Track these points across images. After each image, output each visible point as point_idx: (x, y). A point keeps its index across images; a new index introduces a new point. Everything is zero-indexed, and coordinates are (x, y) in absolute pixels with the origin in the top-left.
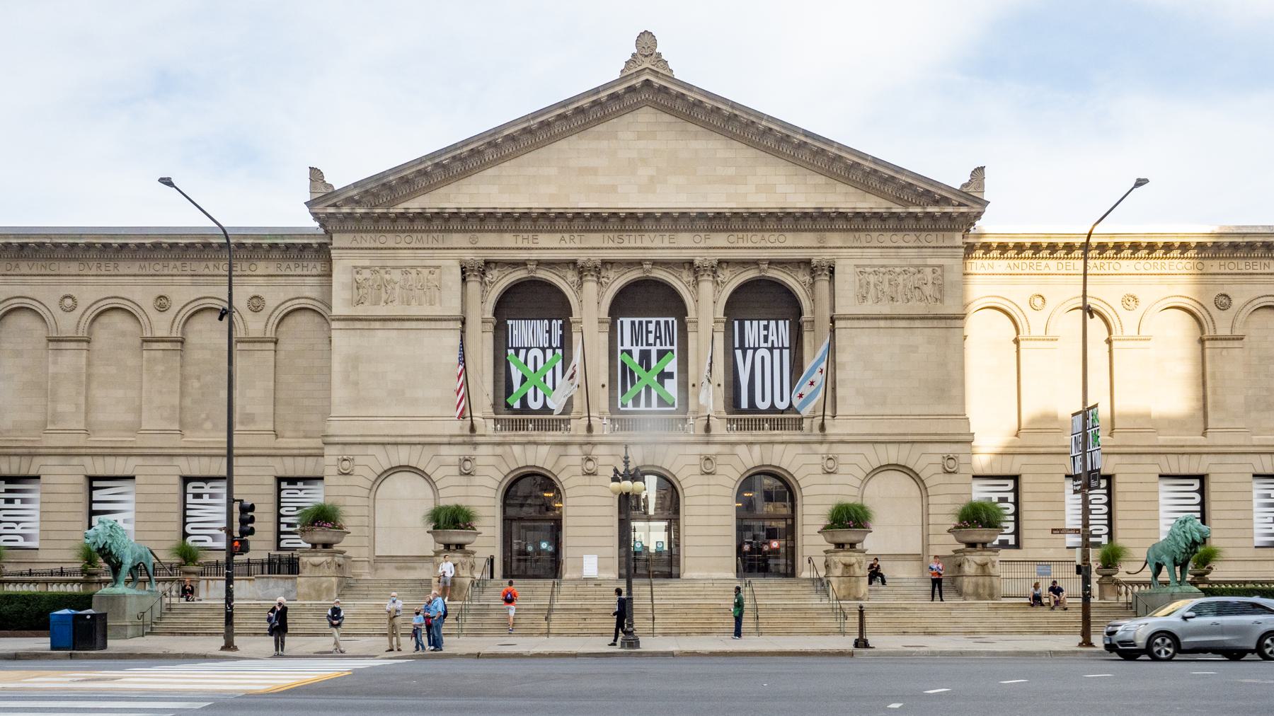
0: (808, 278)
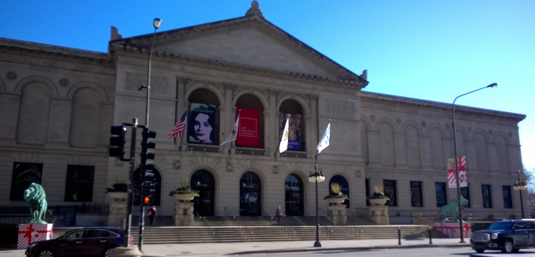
0: (308, 101)
